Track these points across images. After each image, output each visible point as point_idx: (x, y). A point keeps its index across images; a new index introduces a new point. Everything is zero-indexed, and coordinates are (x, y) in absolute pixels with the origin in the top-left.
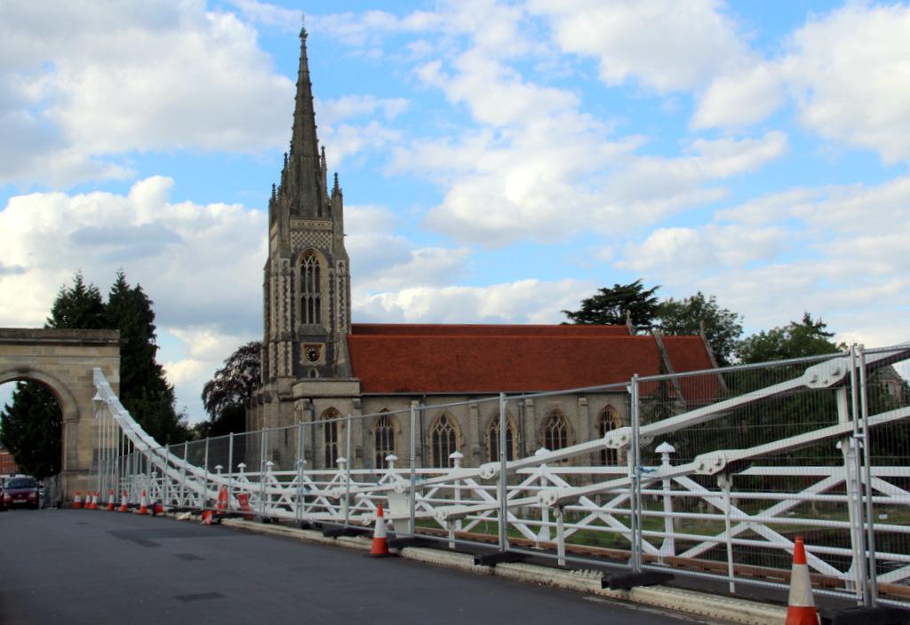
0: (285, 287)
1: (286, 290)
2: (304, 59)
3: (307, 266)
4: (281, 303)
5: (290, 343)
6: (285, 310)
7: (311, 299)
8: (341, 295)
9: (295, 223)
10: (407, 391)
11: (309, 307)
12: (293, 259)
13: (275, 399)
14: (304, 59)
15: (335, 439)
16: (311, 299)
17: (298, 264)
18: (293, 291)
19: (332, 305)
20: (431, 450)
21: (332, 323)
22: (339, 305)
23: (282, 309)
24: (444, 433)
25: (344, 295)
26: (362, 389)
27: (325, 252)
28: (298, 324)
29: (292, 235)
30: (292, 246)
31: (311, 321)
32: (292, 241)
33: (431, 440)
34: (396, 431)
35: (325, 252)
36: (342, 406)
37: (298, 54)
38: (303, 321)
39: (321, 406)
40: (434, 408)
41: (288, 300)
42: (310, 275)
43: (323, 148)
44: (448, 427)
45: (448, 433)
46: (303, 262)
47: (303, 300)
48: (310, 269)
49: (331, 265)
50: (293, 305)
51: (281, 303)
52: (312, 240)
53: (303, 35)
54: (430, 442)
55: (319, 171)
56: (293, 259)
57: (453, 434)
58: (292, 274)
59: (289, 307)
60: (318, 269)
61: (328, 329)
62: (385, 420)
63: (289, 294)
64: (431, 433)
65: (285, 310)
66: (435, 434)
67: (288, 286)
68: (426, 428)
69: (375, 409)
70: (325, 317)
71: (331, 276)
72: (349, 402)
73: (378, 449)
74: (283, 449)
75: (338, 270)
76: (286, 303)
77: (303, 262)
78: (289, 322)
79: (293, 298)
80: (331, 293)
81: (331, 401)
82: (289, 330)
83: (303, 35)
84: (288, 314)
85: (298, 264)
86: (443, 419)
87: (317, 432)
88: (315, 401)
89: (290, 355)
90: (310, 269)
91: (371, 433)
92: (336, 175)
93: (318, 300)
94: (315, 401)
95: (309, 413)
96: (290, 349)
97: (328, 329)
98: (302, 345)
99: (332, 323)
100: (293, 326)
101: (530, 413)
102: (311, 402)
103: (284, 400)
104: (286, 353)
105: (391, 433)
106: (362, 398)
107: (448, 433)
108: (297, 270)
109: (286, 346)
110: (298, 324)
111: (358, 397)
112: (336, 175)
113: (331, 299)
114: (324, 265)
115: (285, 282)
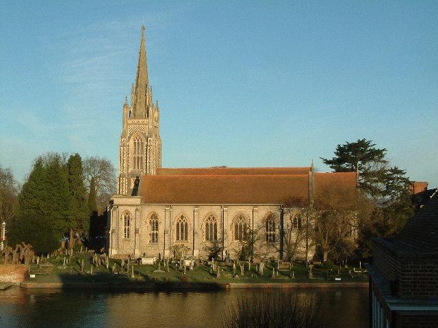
9: (130, 121)
17: (132, 141)
24: (182, 224)
33: (175, 226)
45: (184, 224)
54: (174, 227)
57: (186, 223)
60: (142, 143)
62: (154, 216)
64: (176, 223)
66: (178, 224)
68: (172, 221)
85: (132, 141)
86: (182, 217)
105: (157, 223)
107: (184, 224)
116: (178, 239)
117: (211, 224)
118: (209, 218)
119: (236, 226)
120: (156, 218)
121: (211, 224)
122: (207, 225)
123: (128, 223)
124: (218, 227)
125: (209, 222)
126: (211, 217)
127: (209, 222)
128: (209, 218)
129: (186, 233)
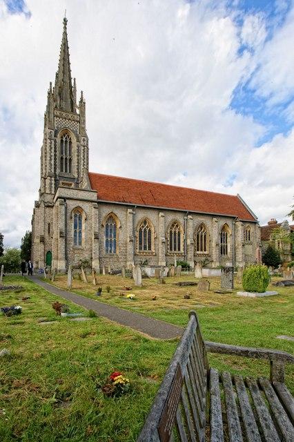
0: (50, 146)
1: (51, 148)
2: (65, 34)
3: (64, 139)
4: (48, 155)
5: (53, 179)
6: (51, 160)
7: (66, 159)
8: (84, 156)
10: (124, 201)
11: (65, 162)
12: (56, 132)
13: (42, 205)
14: (65, 34)
15: (80, 227)
16: (66, 159)
18: (55, 151)
19: (78, 163)
20: (138, 239)
21: (78, 173)
22: (82, 161)
23: (48, 158)
25: (85, 157)
26: (98, 197)
27: (75, 132)
28: (58, 171)
29: (55, 119)
30: (56, 125)
31: (66, 171)
32: (56, 122)
34: (118, 226)
35: (75, 132)
36: (87, 208)
37: (62, 30)
38: (62, 170)
39: (72, 205)
40: (141, 215)
41: (53, 154)
42: (66, 142)
43: (75, 79)
44: (147, 227)
45: (147, 231)
46: (62, 137)
47: (62, 158)
48: (66, 141)
49: (78, 141)
50: (55, 159)
51: (48, 155)
52: (67, 124)
53: (65, 21)
54: (137, 234)
55: (72, 93)
56: (56, 132)
57: (150, 230)
58: (55, 141)
59: (53, 158)
60: (70, 142)
61: (76, 176)
62: (111, 217)
63: (53, 151)
65: (51, 160)
66: (140, 230)
67: (53, 146)
69: (106, 211)
70: (74, 169)
71: (78, 147)
72: (90, 204)
73: (107, 235)
74: (47, 235)
75: (82, 143)
76: (51, 156)
77: (62, 137)
78: (53, 167)
79: (55, 155)
80: (78, 156)
81: (78, 202)
82: (53, 171)
83: (65, 21)
84: (53, 162)
87: (69, 221)
88: (67, 201)
89: (53, 186)
90: (66, 141)
91: (103, 226)
92: (82, 92)
93: (70, 160)
94: (67, 201)
95: (64, 207)
96: (53, 182)
97: (76, 176)
98: (61, 182)
99: (78, 173)
100: (55, 171)
101: (191, 223)
102: (65, 201)
103: (48, 206)
104: (51, 184)
105: (115, 226)
106: (98, 203)
107: (147, 231)
108: (58, 140)
109: (51, 180)
110: (58, 171)
111: (96, 202)
112: (82, 92)
113: (78, 160)
114: (74, 140)
115: (51, 143)
116: (140, 248)
117: (175, 232)
118: (173, 225)
119: (198, 236)
120: (114, 220)
121: (175, 232)
122: (171, 232)
123: (77, 225)
124: (182, 235)
125: (173, 231)
126: (175, 224)
127: (173, 231)
128: (173, 225)
129: (150, 242)
